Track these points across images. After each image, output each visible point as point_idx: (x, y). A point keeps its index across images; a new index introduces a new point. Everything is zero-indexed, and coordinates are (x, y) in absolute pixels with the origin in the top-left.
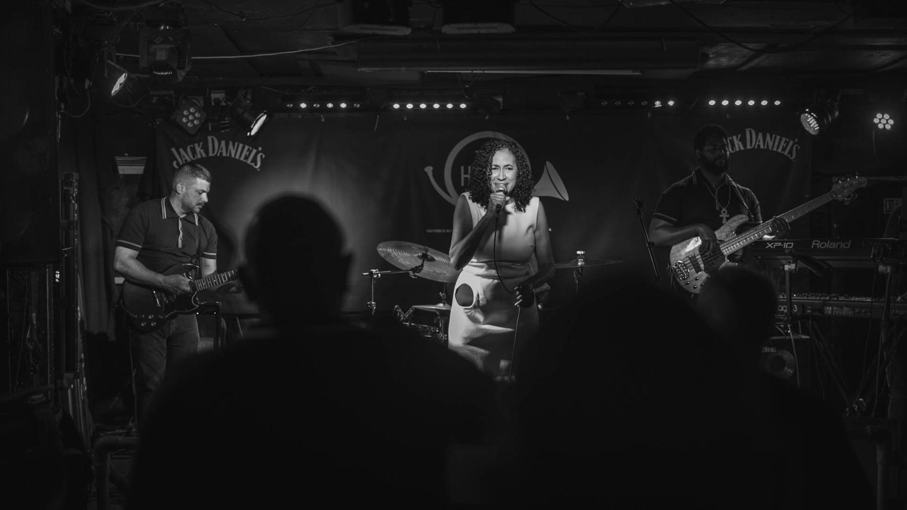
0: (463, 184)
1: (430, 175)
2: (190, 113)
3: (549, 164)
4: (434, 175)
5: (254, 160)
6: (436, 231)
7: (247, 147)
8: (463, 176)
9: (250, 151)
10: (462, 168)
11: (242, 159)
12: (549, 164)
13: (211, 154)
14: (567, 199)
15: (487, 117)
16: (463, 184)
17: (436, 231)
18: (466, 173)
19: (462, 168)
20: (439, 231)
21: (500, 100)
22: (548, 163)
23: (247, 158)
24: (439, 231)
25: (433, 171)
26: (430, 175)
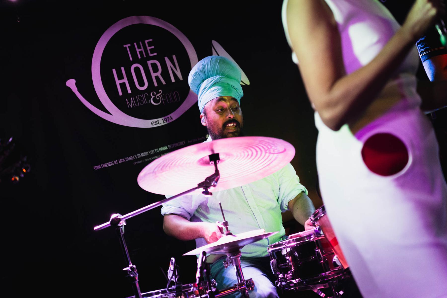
0: (121, 94)
1: (75, 89)
6: (105, 165)
8: (118, 82)
10: (114, 71)
16: (121, 94)
17: (105, 165)
18: (120, 77)
19: (114, 71)
20: (109, 164)
22: (215, 44)
24: (109, 164)
25: (77, 84)
26: (75, 89)
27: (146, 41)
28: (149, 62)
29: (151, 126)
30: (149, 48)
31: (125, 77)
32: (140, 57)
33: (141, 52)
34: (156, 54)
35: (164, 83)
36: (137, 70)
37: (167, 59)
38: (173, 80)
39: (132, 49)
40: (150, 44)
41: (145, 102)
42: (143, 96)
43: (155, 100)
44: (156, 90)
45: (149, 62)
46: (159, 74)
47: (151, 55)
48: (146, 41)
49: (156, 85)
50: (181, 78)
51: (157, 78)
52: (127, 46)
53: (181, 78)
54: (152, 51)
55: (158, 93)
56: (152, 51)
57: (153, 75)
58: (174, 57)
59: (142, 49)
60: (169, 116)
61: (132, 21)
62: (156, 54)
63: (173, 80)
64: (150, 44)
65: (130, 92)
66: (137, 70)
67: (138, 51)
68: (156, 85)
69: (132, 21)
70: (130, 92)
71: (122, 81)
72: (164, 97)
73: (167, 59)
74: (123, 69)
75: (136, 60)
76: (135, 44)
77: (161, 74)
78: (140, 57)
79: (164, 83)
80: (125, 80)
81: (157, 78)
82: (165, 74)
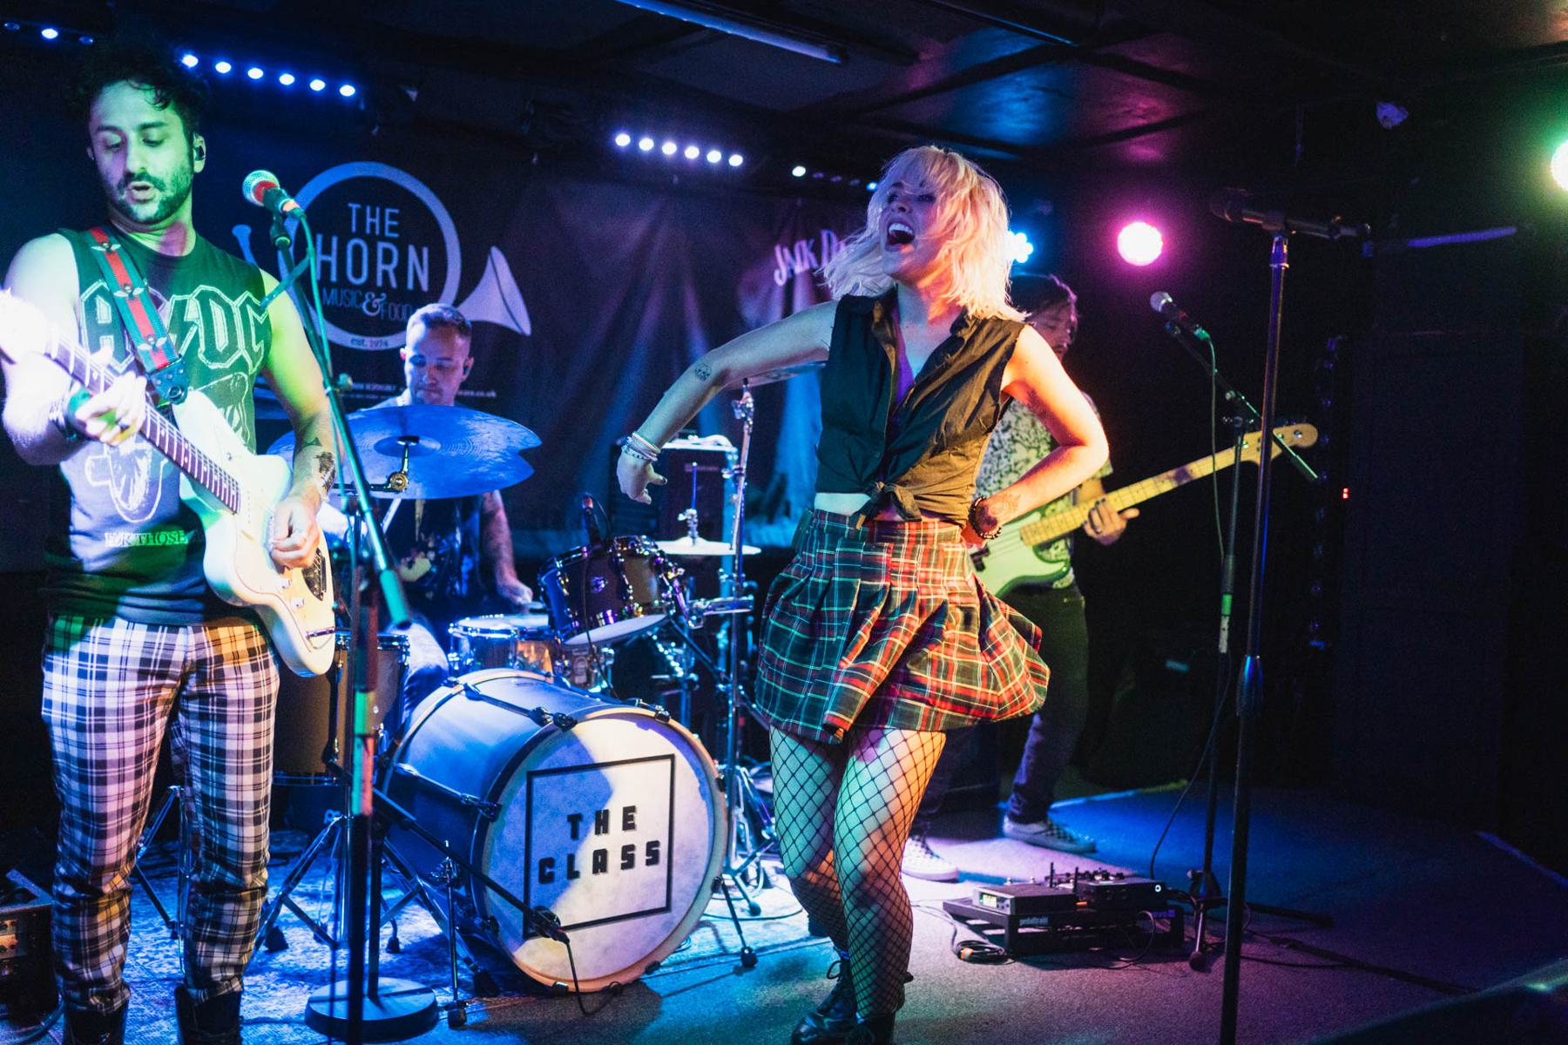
3: (495, 252)
4: (252, 248)
12: (495, 252)
14: (526, 328)
25: (252, 237)
27: (388, 211)
28: (381, 246)
29: (349, 344)
30: (388, 223)
31: (334, 253)
33: (373, 225)
35: (394, 285)
36: (357, 249)
37: (412, 249)
38: (410, 285)
41: (353, 302)
42: (352, 293)
43: (370, 307)
44: (378, 292)
45: (381, 246)
46: (391, 268)
47: (387, 234)
48: (388, 211)
49: (379, 283)
50: (425, 286)
51: (385, 273)
52: (354, 206)
53: (425, 286)
54: (392, 229)
55: (378, 296)
56: (392, 229)
57: (381, 267)
58: (425, 251)
59: (377, 221)
60: (384, 339)
63: (410, 285)
64: (393, 217)
65: (334, 278)
66: (357, 249)
67: (369, 220)
68: (379, 283)
70: (334, 278)
71: (326, 258)
72: (386, 307)
73: (412, 249)
74: (335, 240)
75: (360, 233)
76: (368, 209)
77: (395, 271)
79: (394, 285)
80: (333, 259)
81: (385, 273)
82: (401, 271)
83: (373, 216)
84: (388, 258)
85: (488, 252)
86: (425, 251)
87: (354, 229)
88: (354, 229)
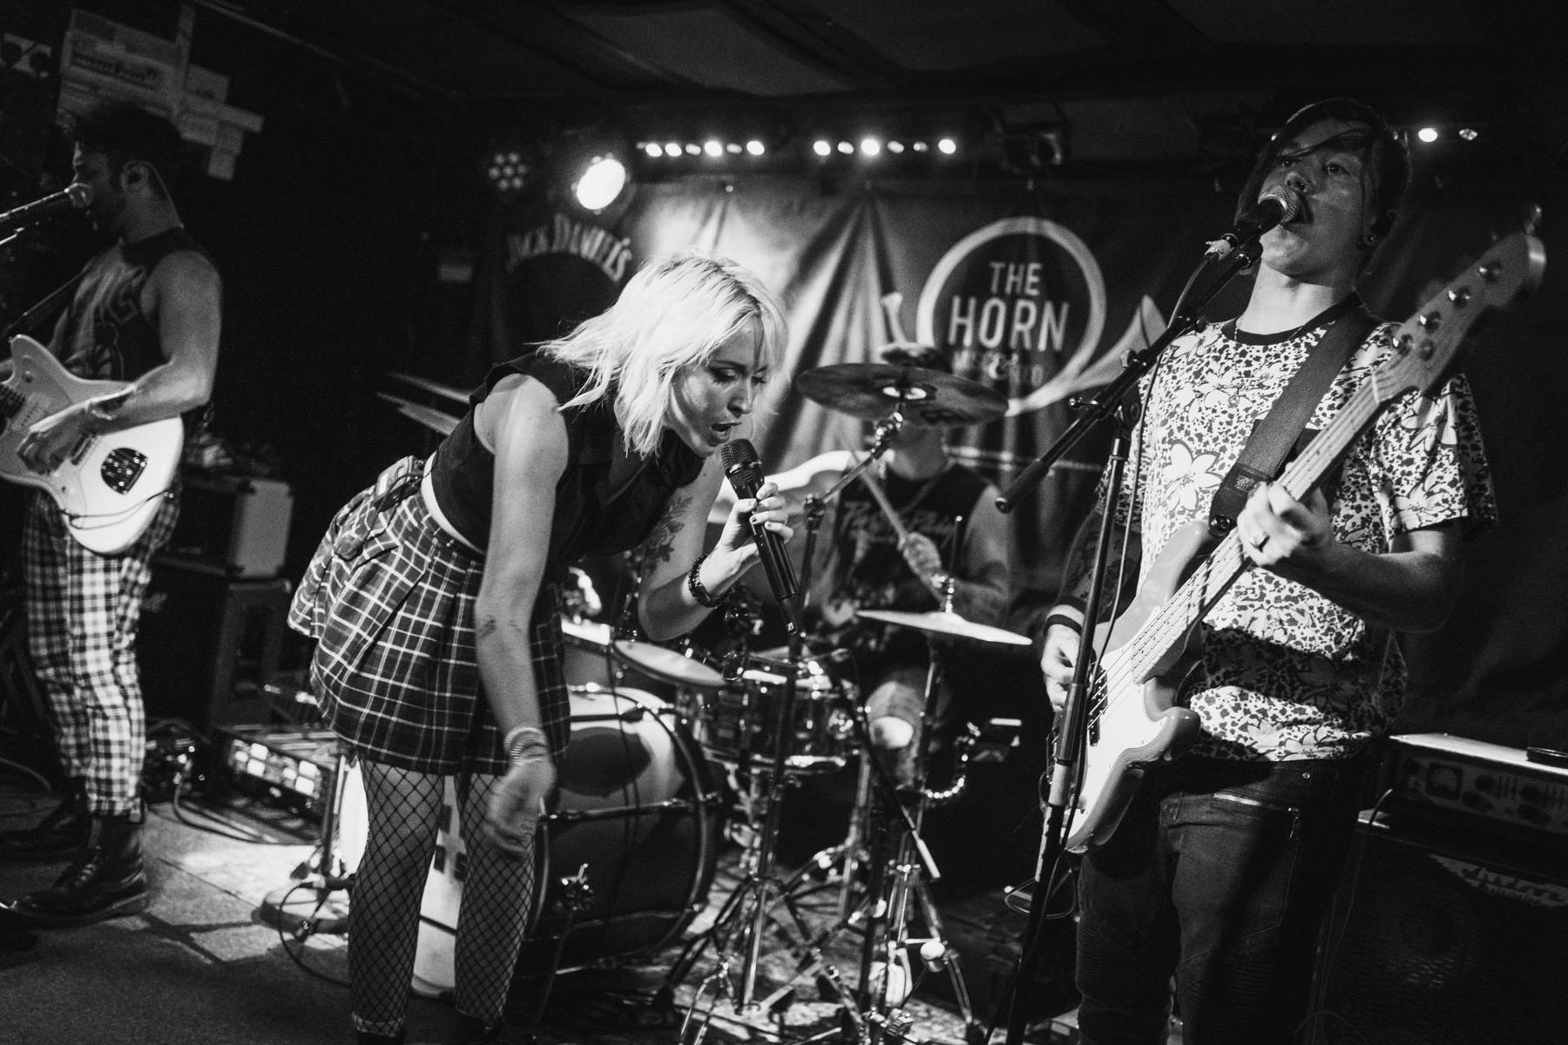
0: (952, 339)
2: (507, 163)
5: (614, 266)
7: (609, 239)
8: (956, 320)
9: (611, 246)
11: (598, 260)
13: (555, 248)
15: (1030, 185)
19: (957, 302)
21: (1051, 136)
23: (605, 258)
30: (1032, 279)
32: (1008, 289)
33: (1014, 284)
34: (1034, 292)
36: (995, 310)
38: (1042, 346)
39: (1004, 274)
40: (1036, 273)
45: (1021, 304)
49: (1013, 343)
51: (1021, 334)
52: (997, 266)
54: (1034, 286)
56: (1034, 286)
57: (1018, 327)
58: (1065, 308)
59: (1019, 279)
61: (1028, 225)
62: (1034, 292)
63: (1042, 346)
64: (1036, 273)
66: (995, 310)
67: (1011, 278)
69: (1028, 225)
74: (972, 303)
75: (1001, 294)
76: (1012, 268)
78: (1008, 289)
79: (1028, 344)
80: (969, 322)
83: (1016, 273)
84: (1025, 319)
85: (1139, 303)
86: (1065, 308)
87: (994, 288)
88: (994, 288)
